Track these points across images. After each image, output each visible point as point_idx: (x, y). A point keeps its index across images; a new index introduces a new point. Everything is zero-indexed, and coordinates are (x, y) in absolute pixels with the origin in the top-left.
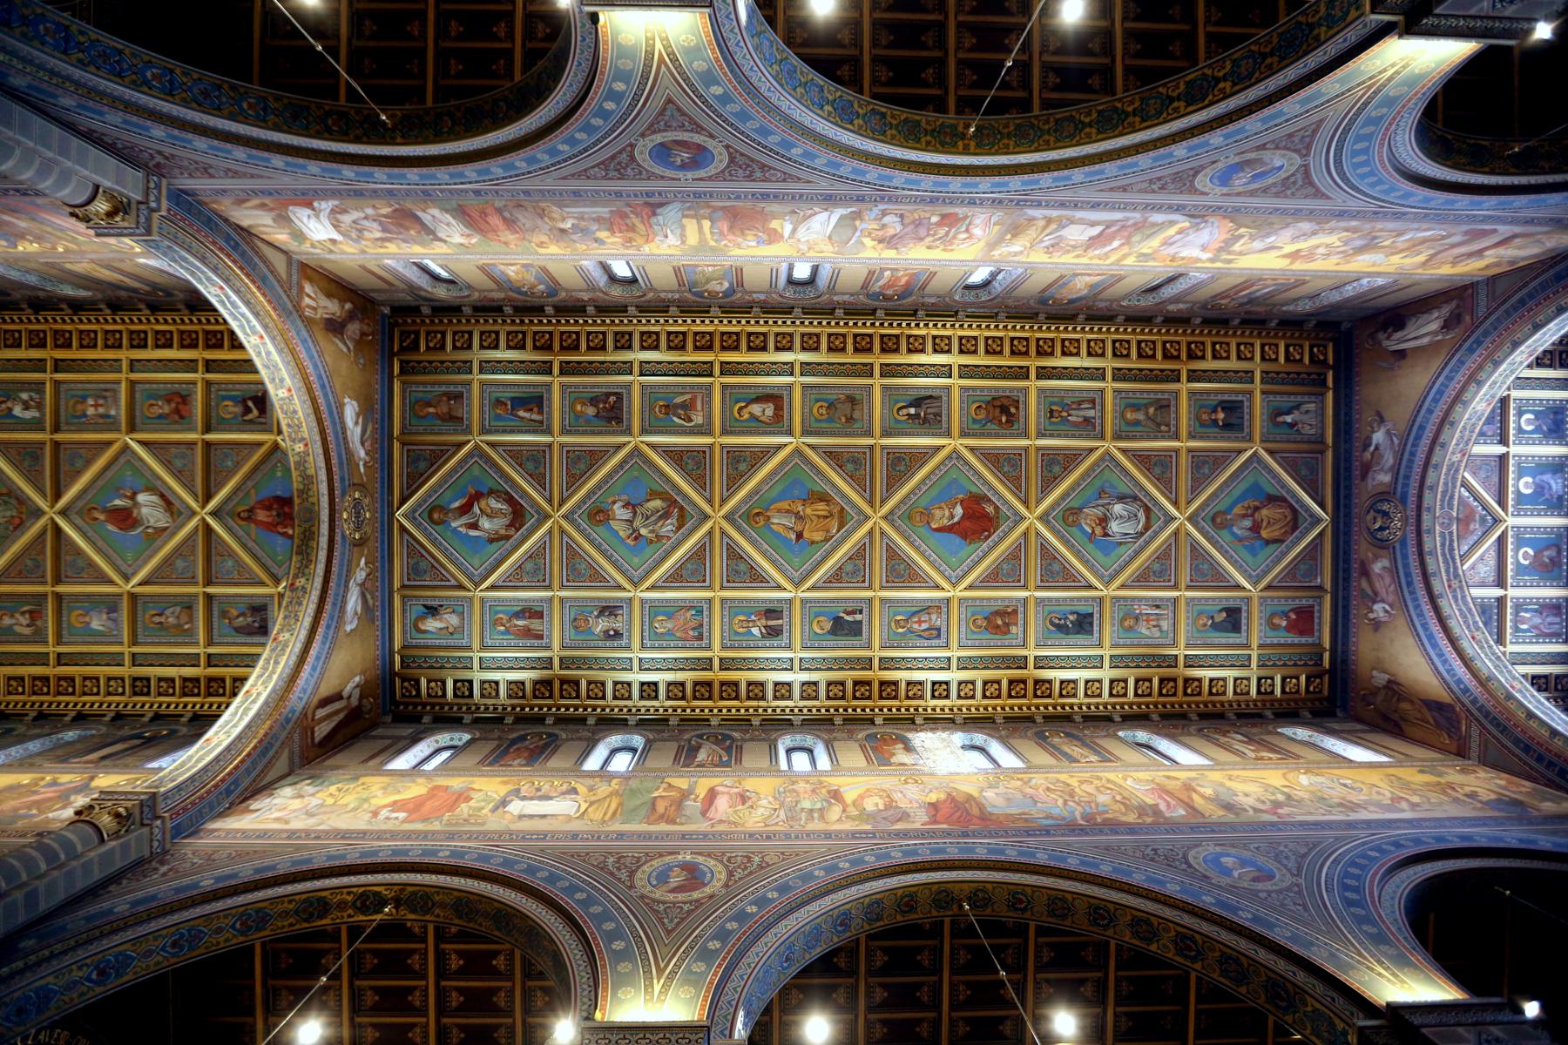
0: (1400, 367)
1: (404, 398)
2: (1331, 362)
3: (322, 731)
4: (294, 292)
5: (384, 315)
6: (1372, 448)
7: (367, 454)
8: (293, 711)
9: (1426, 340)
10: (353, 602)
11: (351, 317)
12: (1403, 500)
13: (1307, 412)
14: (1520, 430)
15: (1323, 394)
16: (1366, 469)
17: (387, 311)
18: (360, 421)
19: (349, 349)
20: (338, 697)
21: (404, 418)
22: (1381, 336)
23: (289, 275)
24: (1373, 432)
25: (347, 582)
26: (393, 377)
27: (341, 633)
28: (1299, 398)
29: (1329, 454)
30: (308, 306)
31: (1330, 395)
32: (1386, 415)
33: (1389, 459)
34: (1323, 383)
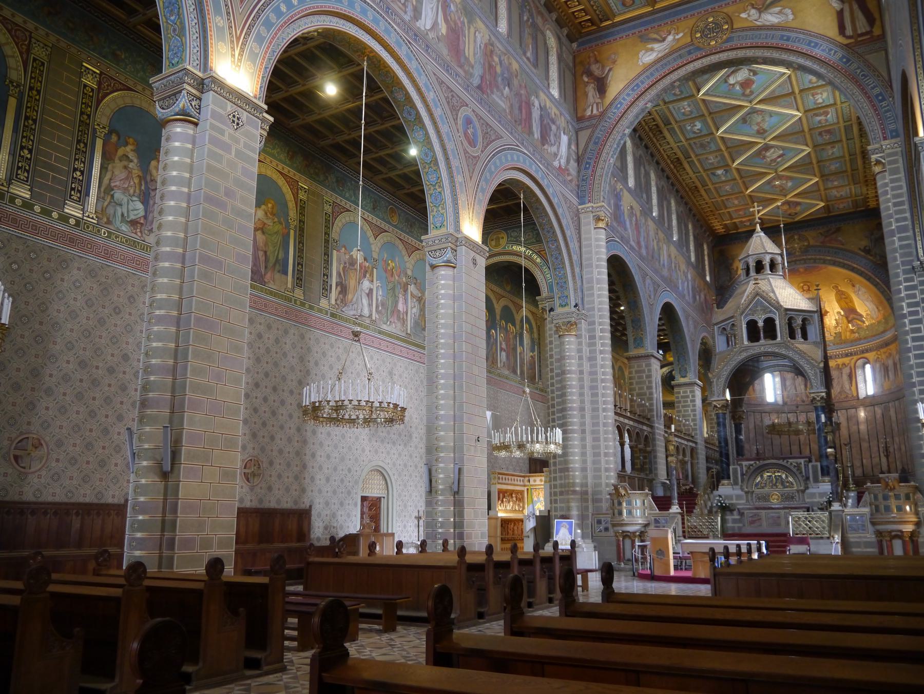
1: (625, 13)
3: (862, 25)
4: (594, 122)
5: (578, 47)
7: (670, 34)
8: (843, 57)
10: (771, 18)
11: (590, 74)
17: (575, 45)
18: (650, 46)
19: (610, 70)
20: (840, 14)
21: (638, 8)
23: (587, 128)
25: (759, 28)
26: (613, 23)
27: (794, 25)
30: (598, 110)
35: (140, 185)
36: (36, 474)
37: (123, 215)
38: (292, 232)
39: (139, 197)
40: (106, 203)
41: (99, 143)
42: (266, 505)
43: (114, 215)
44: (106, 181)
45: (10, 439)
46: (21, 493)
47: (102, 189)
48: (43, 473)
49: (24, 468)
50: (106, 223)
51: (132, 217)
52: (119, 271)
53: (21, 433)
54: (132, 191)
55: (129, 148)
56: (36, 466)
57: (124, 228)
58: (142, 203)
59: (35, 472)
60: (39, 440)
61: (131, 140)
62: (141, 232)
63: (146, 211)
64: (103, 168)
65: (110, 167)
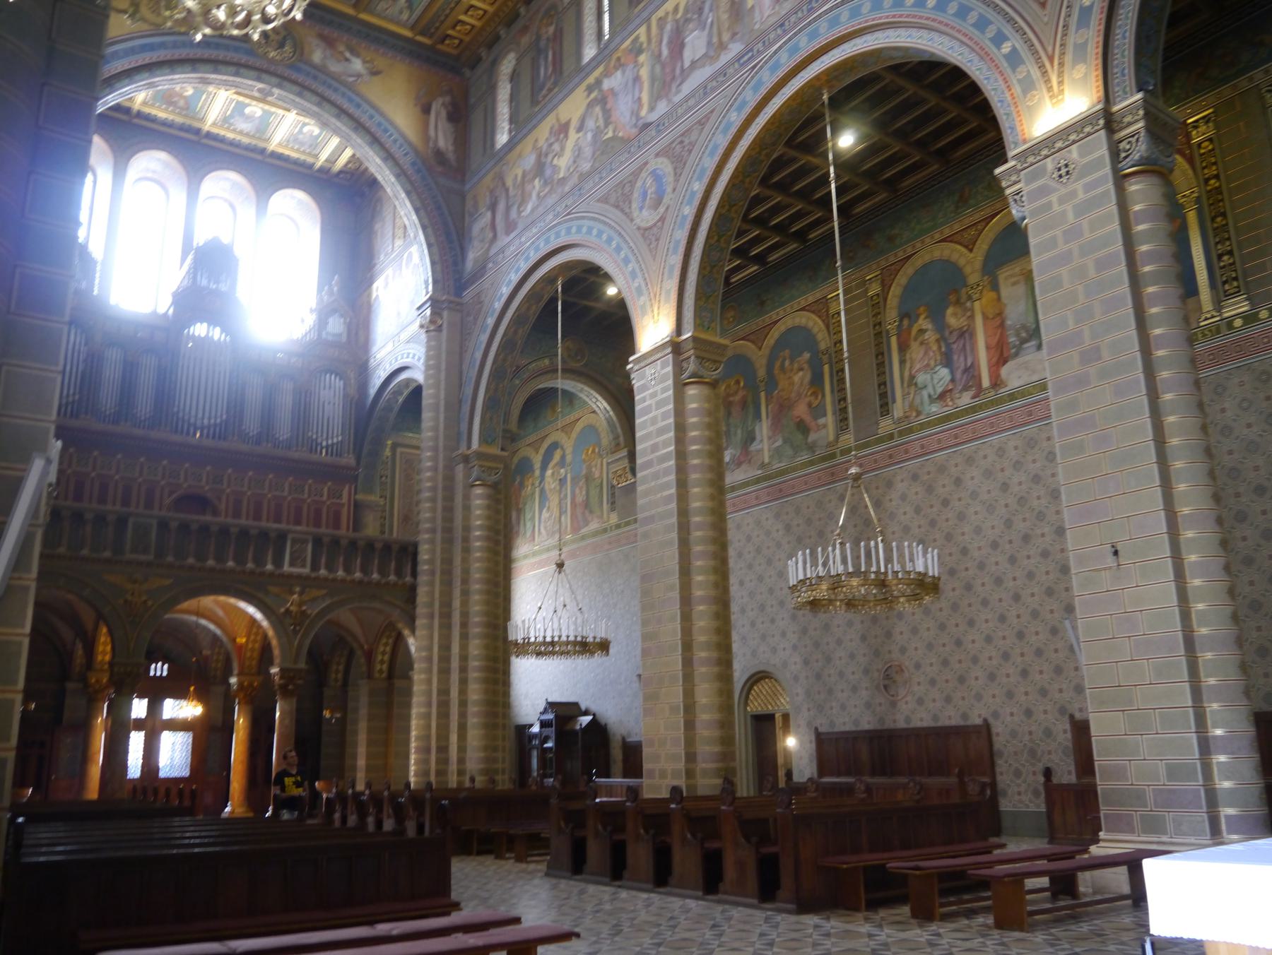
0: (416, 105)
2: (440, 47)
6: (348, 55)
9: (432, 133)
12: (292, 67)
13: (401, 12)
14: (305, 124)
15: (412, 28)
16: (329, 43)
22: (448, 99)
24: (364, 62)
28: (418, 12)
29: (351, 11)
31: (408, 33)
32: (375, 79)
33: (335, 67)
34: (422, 33)
35: (940, 347)
36: (904, 700)
37: (930, 396)
38: (1192, 217)
39: (941, 364)
40: (912, 396)
41: (894, 340)
42: (889, 725)
43: (922, 403)
44: (907, 374)
45: (878, 670)
46: (895, 721)
47: (905, 385)
48: (909, 698)
49: (893, 696)
50: (917, 416)
51: (939, 390)
52: (965, 450)
53: (886, 663)
54: (932, 363)
55: (921, 321)
56: (902, 692)
57: (934, 408)
58: (946, 366)
59: (903, 698)
60: (899, 666)
61: (922, 309)
62: (952, 400)
63: (952, 373)
64: (902, 362)
65: (908, 356)
